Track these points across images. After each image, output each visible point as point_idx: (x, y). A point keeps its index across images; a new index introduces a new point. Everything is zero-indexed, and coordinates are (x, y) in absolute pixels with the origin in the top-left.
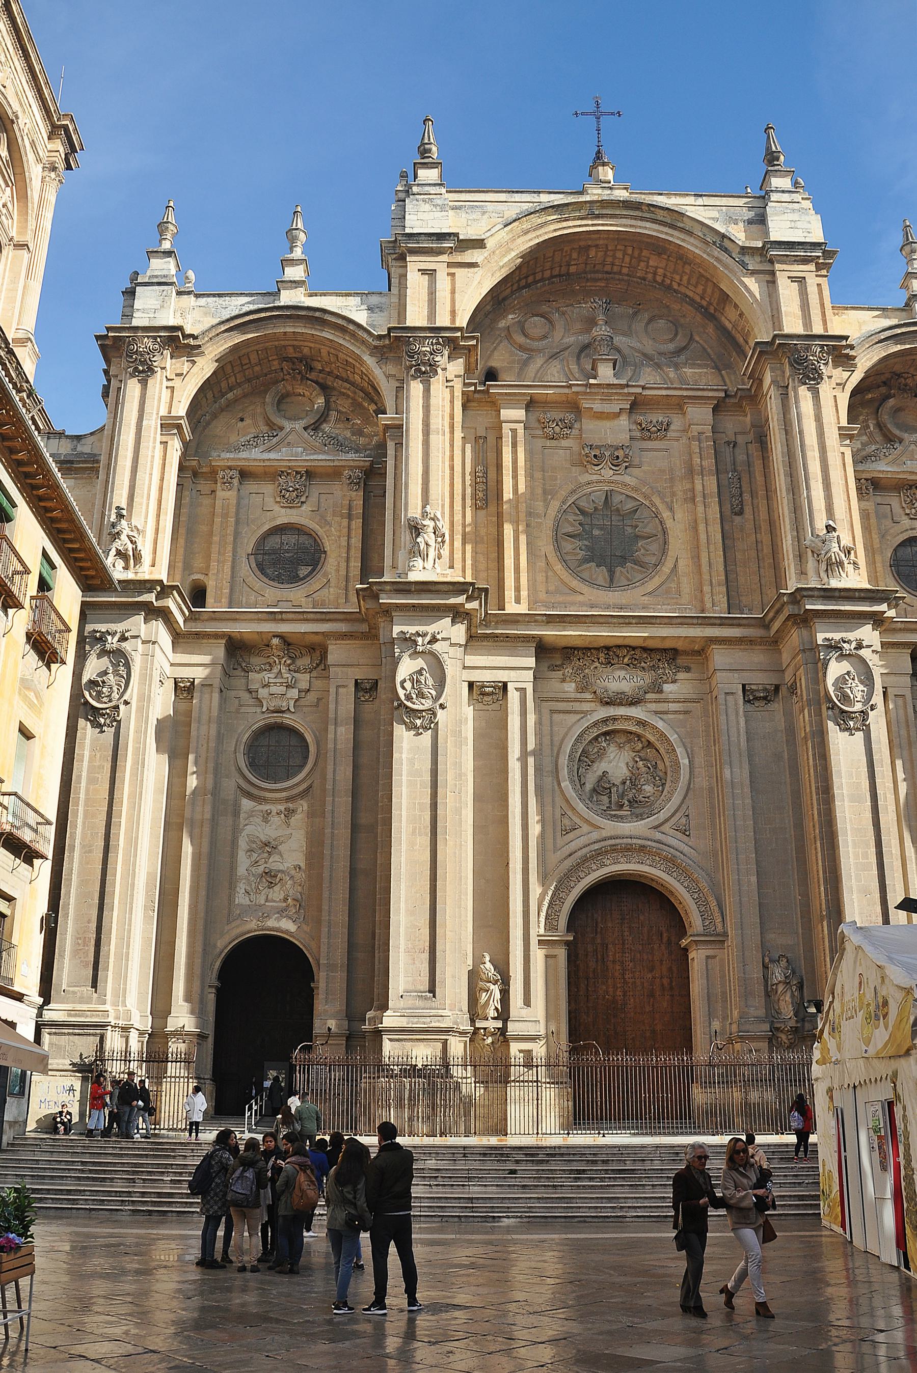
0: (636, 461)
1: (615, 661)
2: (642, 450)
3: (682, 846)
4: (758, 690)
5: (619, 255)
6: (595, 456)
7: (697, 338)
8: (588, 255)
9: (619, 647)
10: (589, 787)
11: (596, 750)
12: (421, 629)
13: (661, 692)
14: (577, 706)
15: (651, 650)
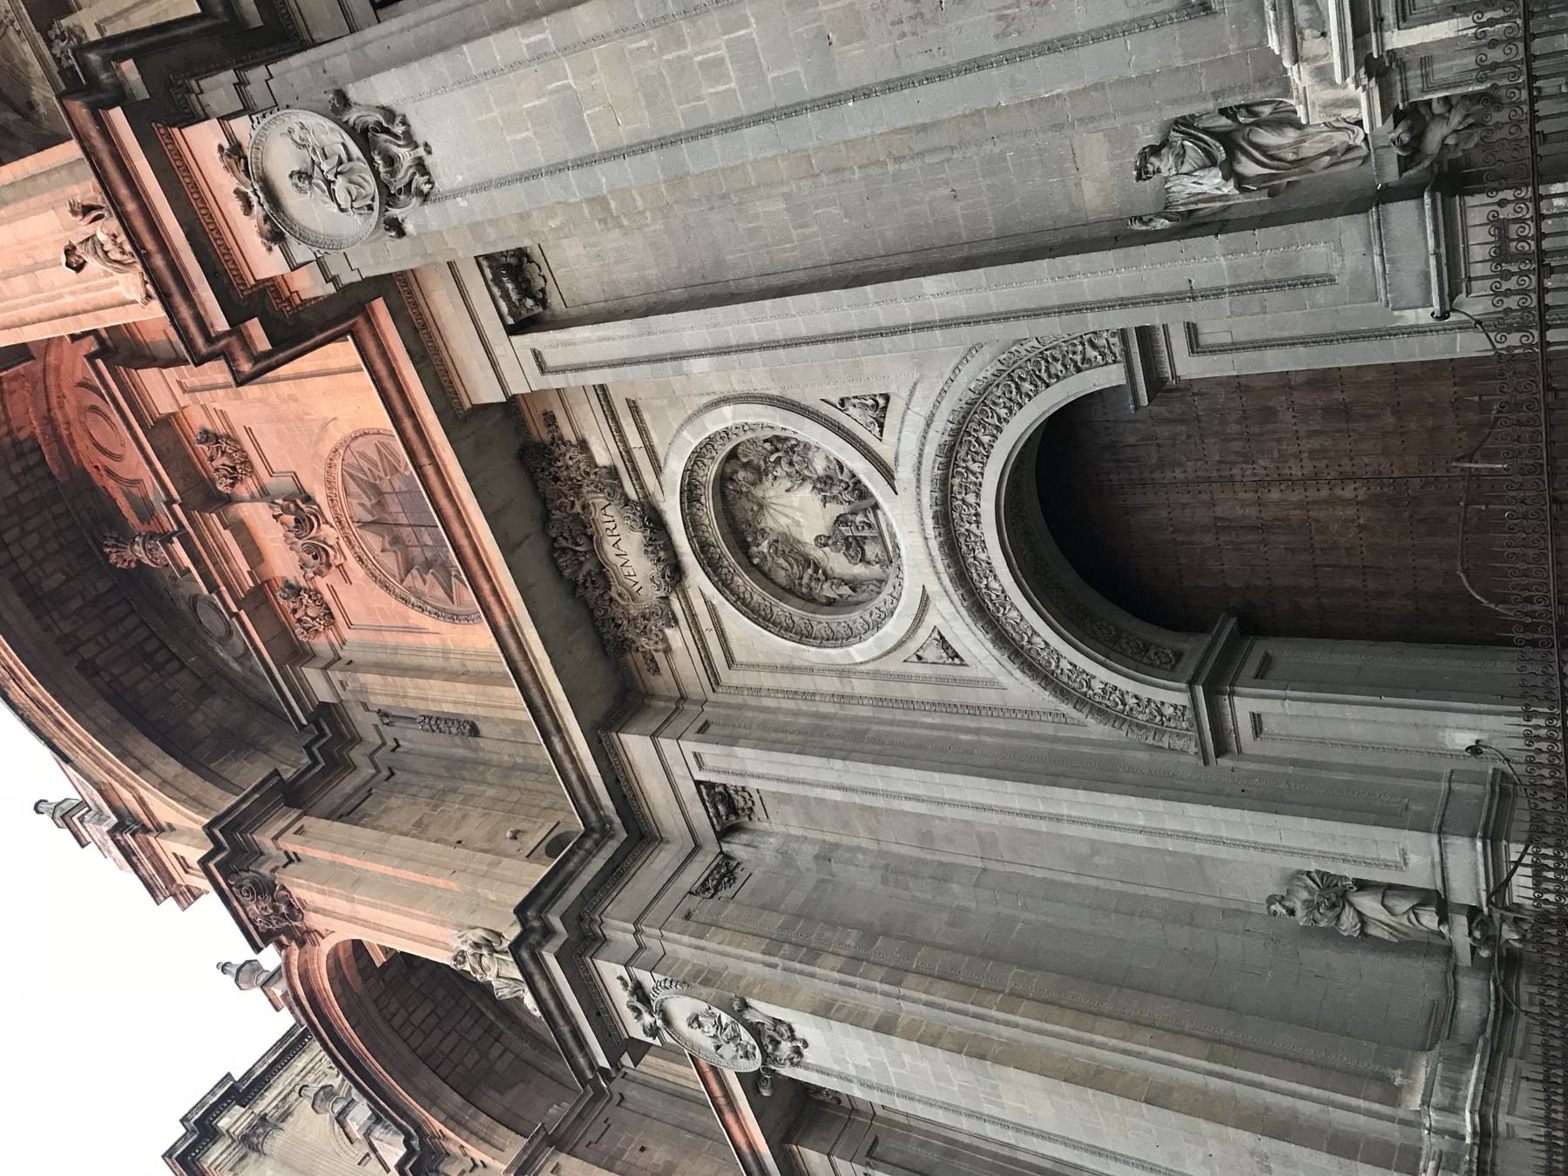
0: (287, 484)
1: (587, 567)
2: (271, 473)
3: (916, 420)
4: (506, 295)
5: (33, 539)
6: (315, 557)
7: (79, 376)
8: (65, 582)
9: (559, 571)
10: (859, 570)
11: (781, 561)
12: (628, 1015)
13: (613, 472)
14: (705, 622)
15: (544, 501)
